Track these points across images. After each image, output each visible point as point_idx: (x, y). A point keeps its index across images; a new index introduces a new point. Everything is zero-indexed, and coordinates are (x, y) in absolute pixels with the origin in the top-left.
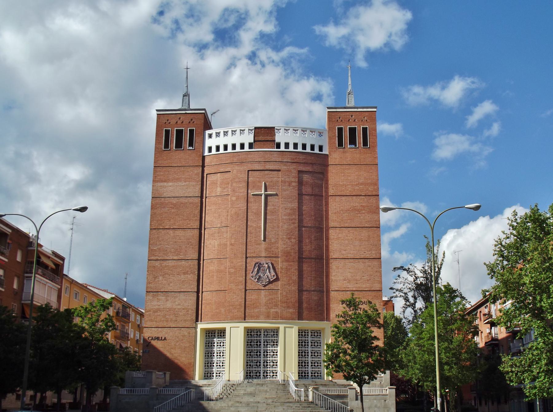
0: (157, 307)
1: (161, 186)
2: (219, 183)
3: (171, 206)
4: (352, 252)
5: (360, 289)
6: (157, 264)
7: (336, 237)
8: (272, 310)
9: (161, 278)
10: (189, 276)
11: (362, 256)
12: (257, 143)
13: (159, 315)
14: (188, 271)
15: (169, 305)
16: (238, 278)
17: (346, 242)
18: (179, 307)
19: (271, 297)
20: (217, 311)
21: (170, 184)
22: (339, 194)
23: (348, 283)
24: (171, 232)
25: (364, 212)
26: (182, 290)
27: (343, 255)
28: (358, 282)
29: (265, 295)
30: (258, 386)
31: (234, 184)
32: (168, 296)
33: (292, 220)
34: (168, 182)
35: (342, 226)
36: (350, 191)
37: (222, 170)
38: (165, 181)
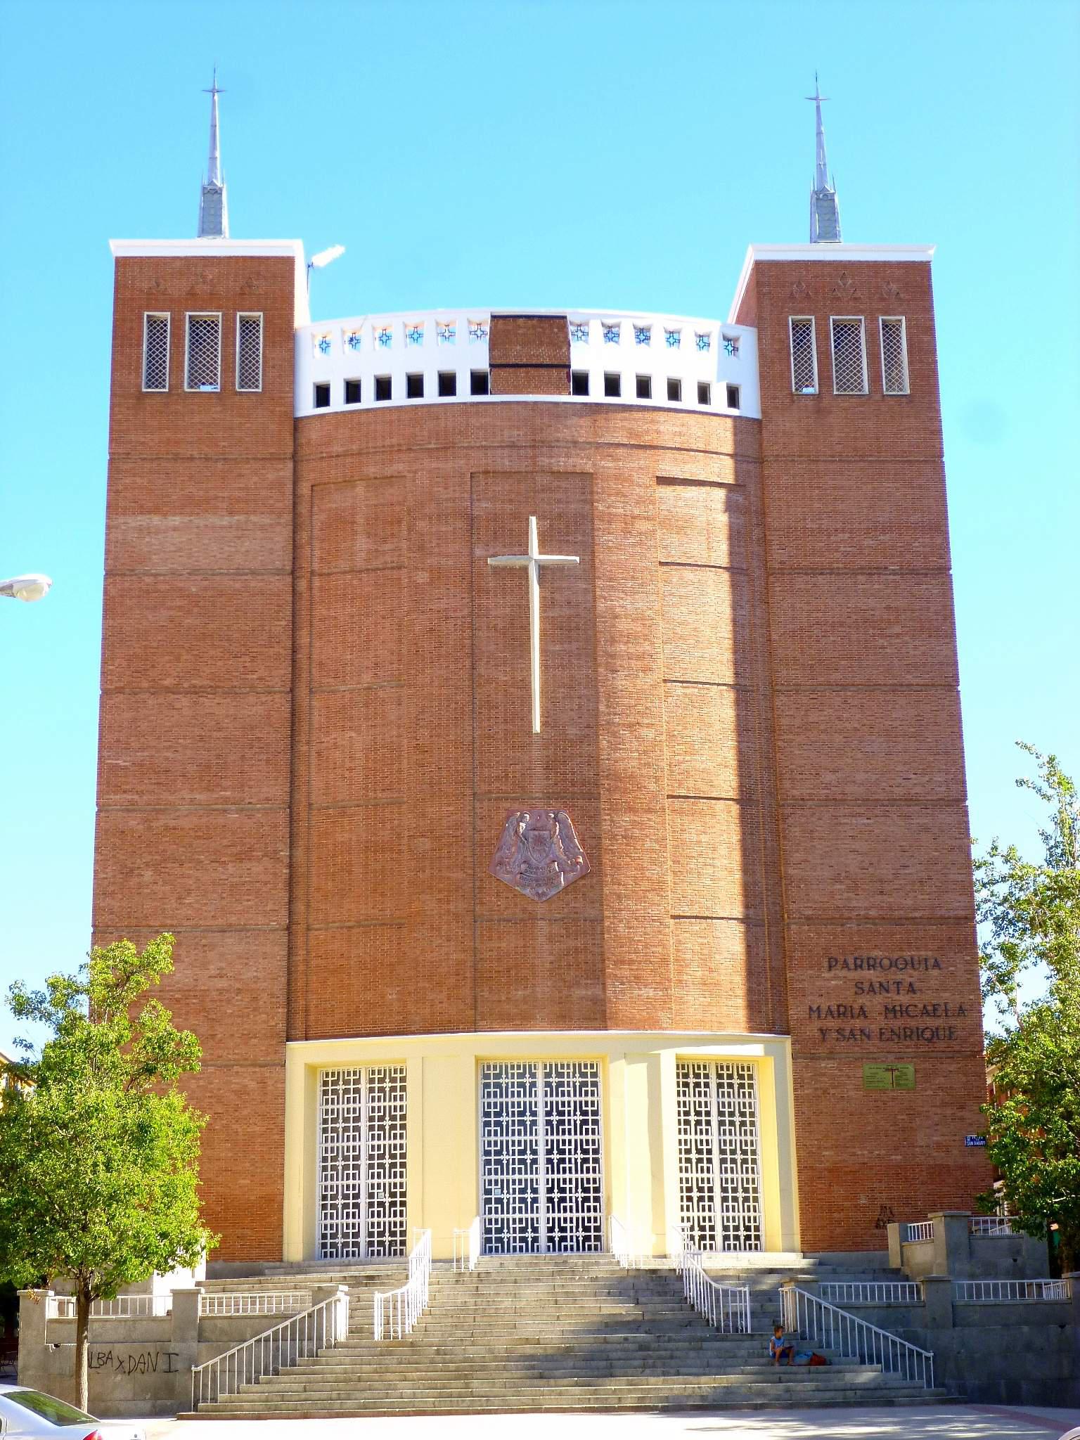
1: (140, 529)
2: (360, 519)
4: (860, 777)
7: (797, 722)
8: (579, 992)
9: (148, 875)
10: (257, 868)
12: (503, 373)
16: (445, 874)
17: (838, 739)
18: (222, 984)
19: (571, 943)
20: (369, 996)
21: (176, 520)
23: (849, 889)
25: (897, 629)
27: (827, 786)
31: (422, 525)
34: (165, 515)
36: (846, 554)
37: (371, 470)
38: (156, 510)
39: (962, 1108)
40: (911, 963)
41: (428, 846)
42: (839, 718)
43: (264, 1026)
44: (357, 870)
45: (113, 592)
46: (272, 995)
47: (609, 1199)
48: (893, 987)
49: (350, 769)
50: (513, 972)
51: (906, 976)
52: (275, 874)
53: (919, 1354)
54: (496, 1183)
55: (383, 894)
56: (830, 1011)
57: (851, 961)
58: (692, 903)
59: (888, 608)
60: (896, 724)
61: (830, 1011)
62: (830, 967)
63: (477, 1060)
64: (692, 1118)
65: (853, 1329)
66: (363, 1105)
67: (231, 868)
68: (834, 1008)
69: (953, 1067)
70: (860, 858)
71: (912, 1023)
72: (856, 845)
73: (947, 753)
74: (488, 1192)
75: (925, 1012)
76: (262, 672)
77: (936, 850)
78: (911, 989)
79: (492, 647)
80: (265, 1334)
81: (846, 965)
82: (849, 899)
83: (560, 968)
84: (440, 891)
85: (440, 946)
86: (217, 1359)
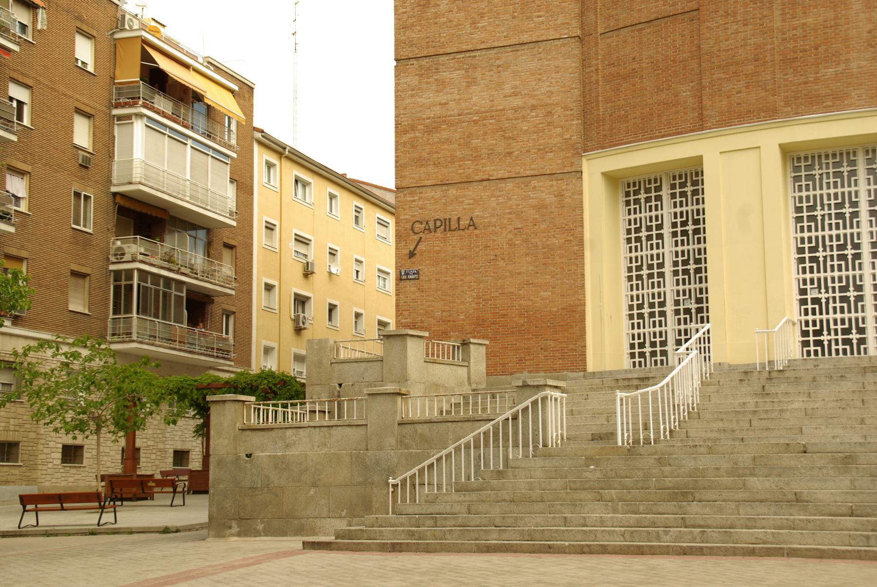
0: (438, 111)
13: (449, 141)
15: (479, 98)
18: (517, 102)
20: (663, 96)
26: (525, 38)
32: (475, 67)
43: (559, 139)
46: (566, 108)
50: (821, 49)
54: (812, 282)
63: (780, 145)
66: (665, 212)
74: (803, 292)
80: (463, 441)
85: (737, 32)
86: (415, 470)
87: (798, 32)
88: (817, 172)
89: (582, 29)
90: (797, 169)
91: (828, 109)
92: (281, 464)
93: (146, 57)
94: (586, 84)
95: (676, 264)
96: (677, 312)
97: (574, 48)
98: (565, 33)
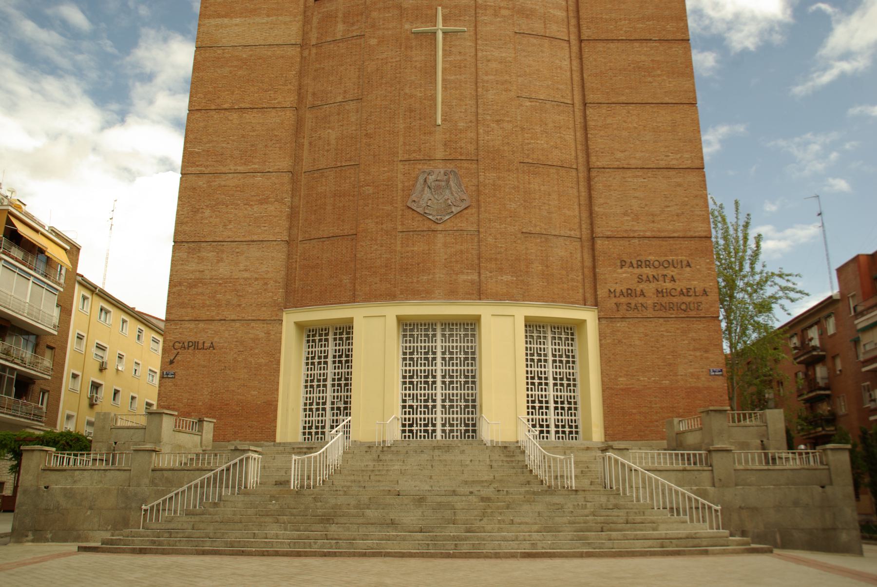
0: (198, 275)
1: (216, 26)
3: (235, 63)
4: (638, 155)
5: (663, 235)
6: (201, 182)
7: (600, 124)
9: (208, 212)
10: (271, 208)
11: (662, 164)
13: (202, 294)
14: (268, 197)
15: (224, 270)
17: (625, 134)
18: (246, 275)
19: (458, 247)
21: (238, 20)
22: (603, 37)
24: (235, 116)
25: (659, 72)
26: (255, 238)
27: (618, 160)
28: (656, 219)
29: (445, 245)
30: (437, 452)
32: (223, 251)
33: (502, 84)
34: (231, 18)
35: (614, 100)
36: (626, 32)
38: (225, 16)
39: (706, 351)
40: (672, 264)
41: (371, 192)
42: (625, 122)
44: (329, 208)
45: (199, 58)
46: (276, 282)
47: (481, 406)
48: (661, 278)
49: (328, 151)
51: (670, 272)
52: (281, 211)
53: (710, 508)
55: (343, 221)
56: (622, 293)
57: (634, 262)
58: (536, 226)
59: (652, 61)
60: (660, 124)
61: (622, 293)
62: (622, 267)
64: (534, 357)
65: (657, 488)
66: (330, 348)
67: (256, 208)
68: (624, 291)
69: (701, 326)
70: (639, 202)
71: (675, 300)
72: (637, 194)
73: (691, 141)
74: (404, 401)
75: (682, 293)
76: (279, 100)
77: (686, 197)
78: (673, 279)
79: (413, 78)
81: (631, 265)
82: (633, 225)
83: (451, 262)
84: (377, 218)
85: (376, 250)
87: (409, 254)
88: (415, 333)
89: (289, 236)
90: (405, 330)
91: (423, 298)
92: (69, 494)
93: (9, 222)
94: (289, 268)
95: (334, 380)
96: (333, 409)
97: (284, 247)
98: (279, 238)
